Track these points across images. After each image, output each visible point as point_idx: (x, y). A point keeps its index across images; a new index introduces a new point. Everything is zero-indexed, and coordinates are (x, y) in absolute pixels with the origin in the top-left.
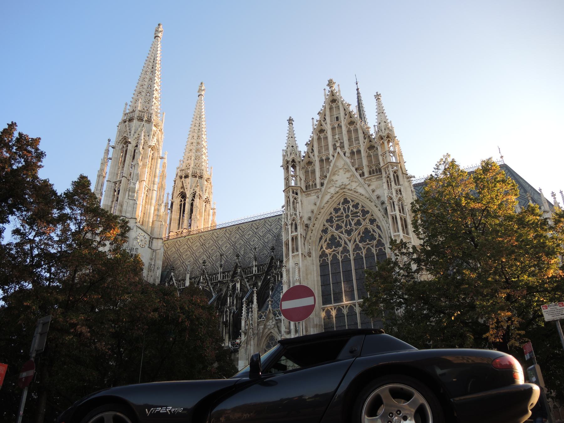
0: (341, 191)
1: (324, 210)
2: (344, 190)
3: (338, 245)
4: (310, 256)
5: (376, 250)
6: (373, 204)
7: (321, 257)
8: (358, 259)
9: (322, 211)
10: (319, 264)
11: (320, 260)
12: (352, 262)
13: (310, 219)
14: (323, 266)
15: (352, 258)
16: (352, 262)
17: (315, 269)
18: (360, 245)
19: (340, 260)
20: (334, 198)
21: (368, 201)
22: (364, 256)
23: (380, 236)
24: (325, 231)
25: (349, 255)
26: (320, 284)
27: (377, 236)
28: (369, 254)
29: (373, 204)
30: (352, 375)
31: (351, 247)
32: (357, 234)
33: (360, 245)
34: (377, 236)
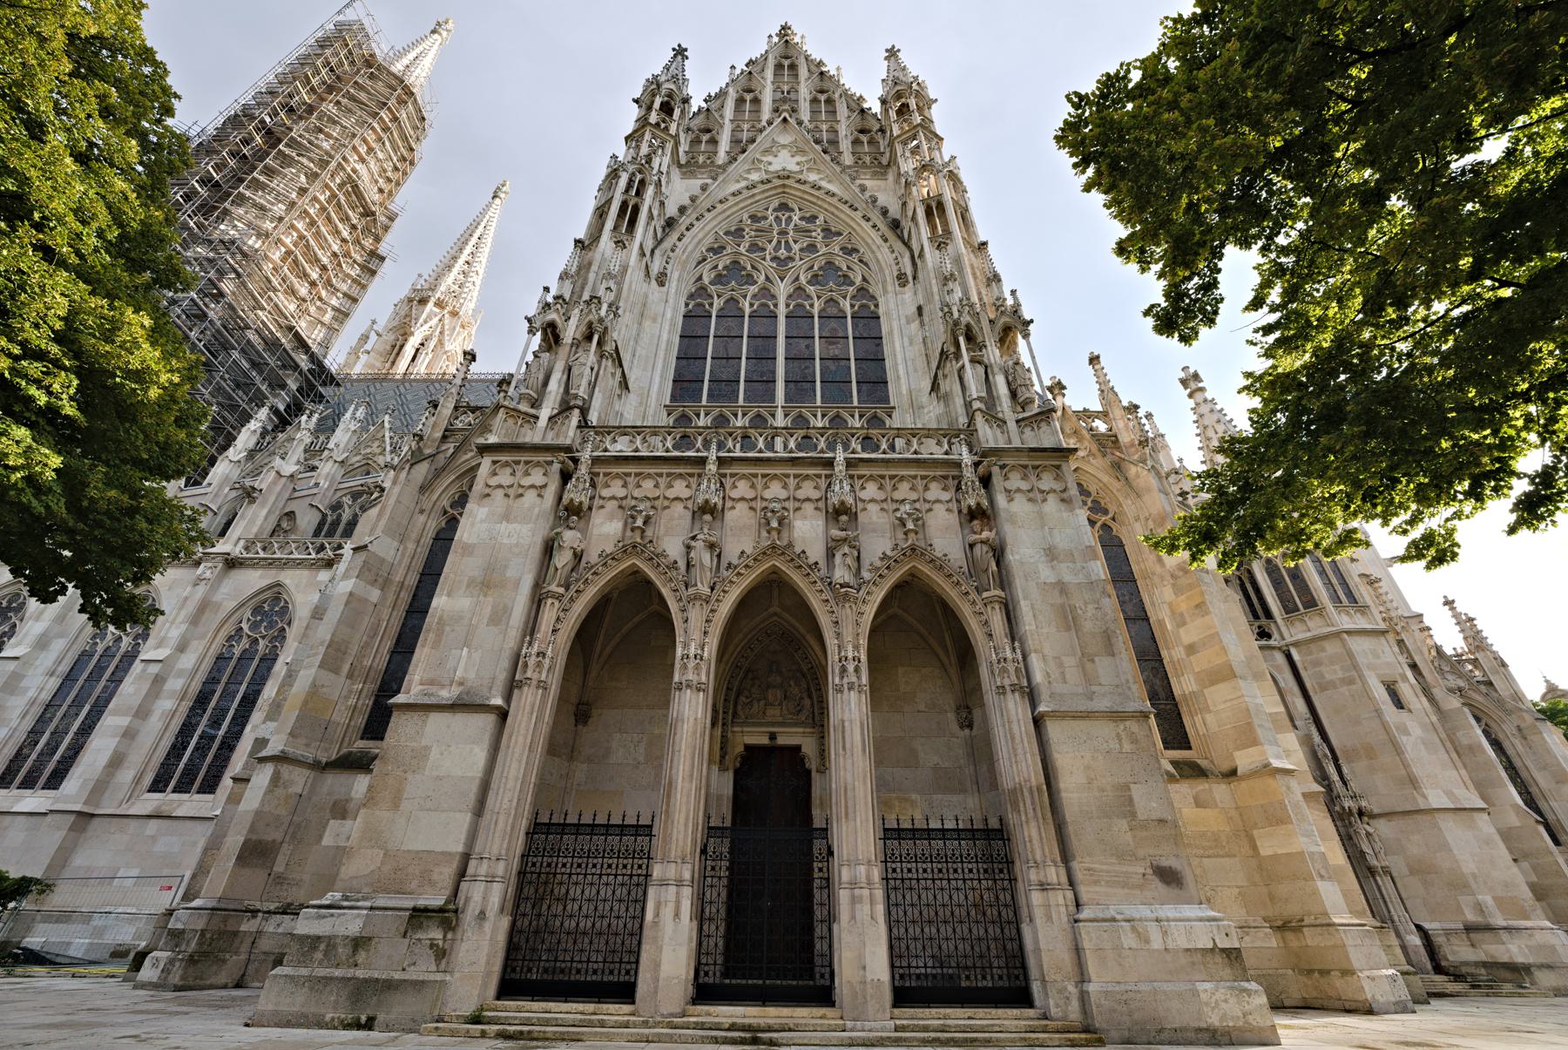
0: (777, 182)
1: (725, 206)
2: (787, 182)
3: (750, 280)
4: (662, 284)
5: (852, 306)
6: (859, 214)
7: (691, 296)
8: (798, 316)
9: (720, 207)
10: (682, 310)
11: (687, 305)
12: (782, 321)
13: (682, 210)
14: (694, 317)
15: (782, 311)
16: (782, 321)
17: (669, 315)
18: (811, 289)
19: (747, 311)
20: (755, 191)
21: (845, 208)
22: (816, 312)
23: (864, 279)
24: (717, 250)
25: (776, 305)
26: (675, 353)
27: (858, 281)
28: (832, 316)
29: (859, 214)
30: (726, 607)
31: (782, 290)
32: (805, 267)
33: (811, 289)
34: (858, 281)
